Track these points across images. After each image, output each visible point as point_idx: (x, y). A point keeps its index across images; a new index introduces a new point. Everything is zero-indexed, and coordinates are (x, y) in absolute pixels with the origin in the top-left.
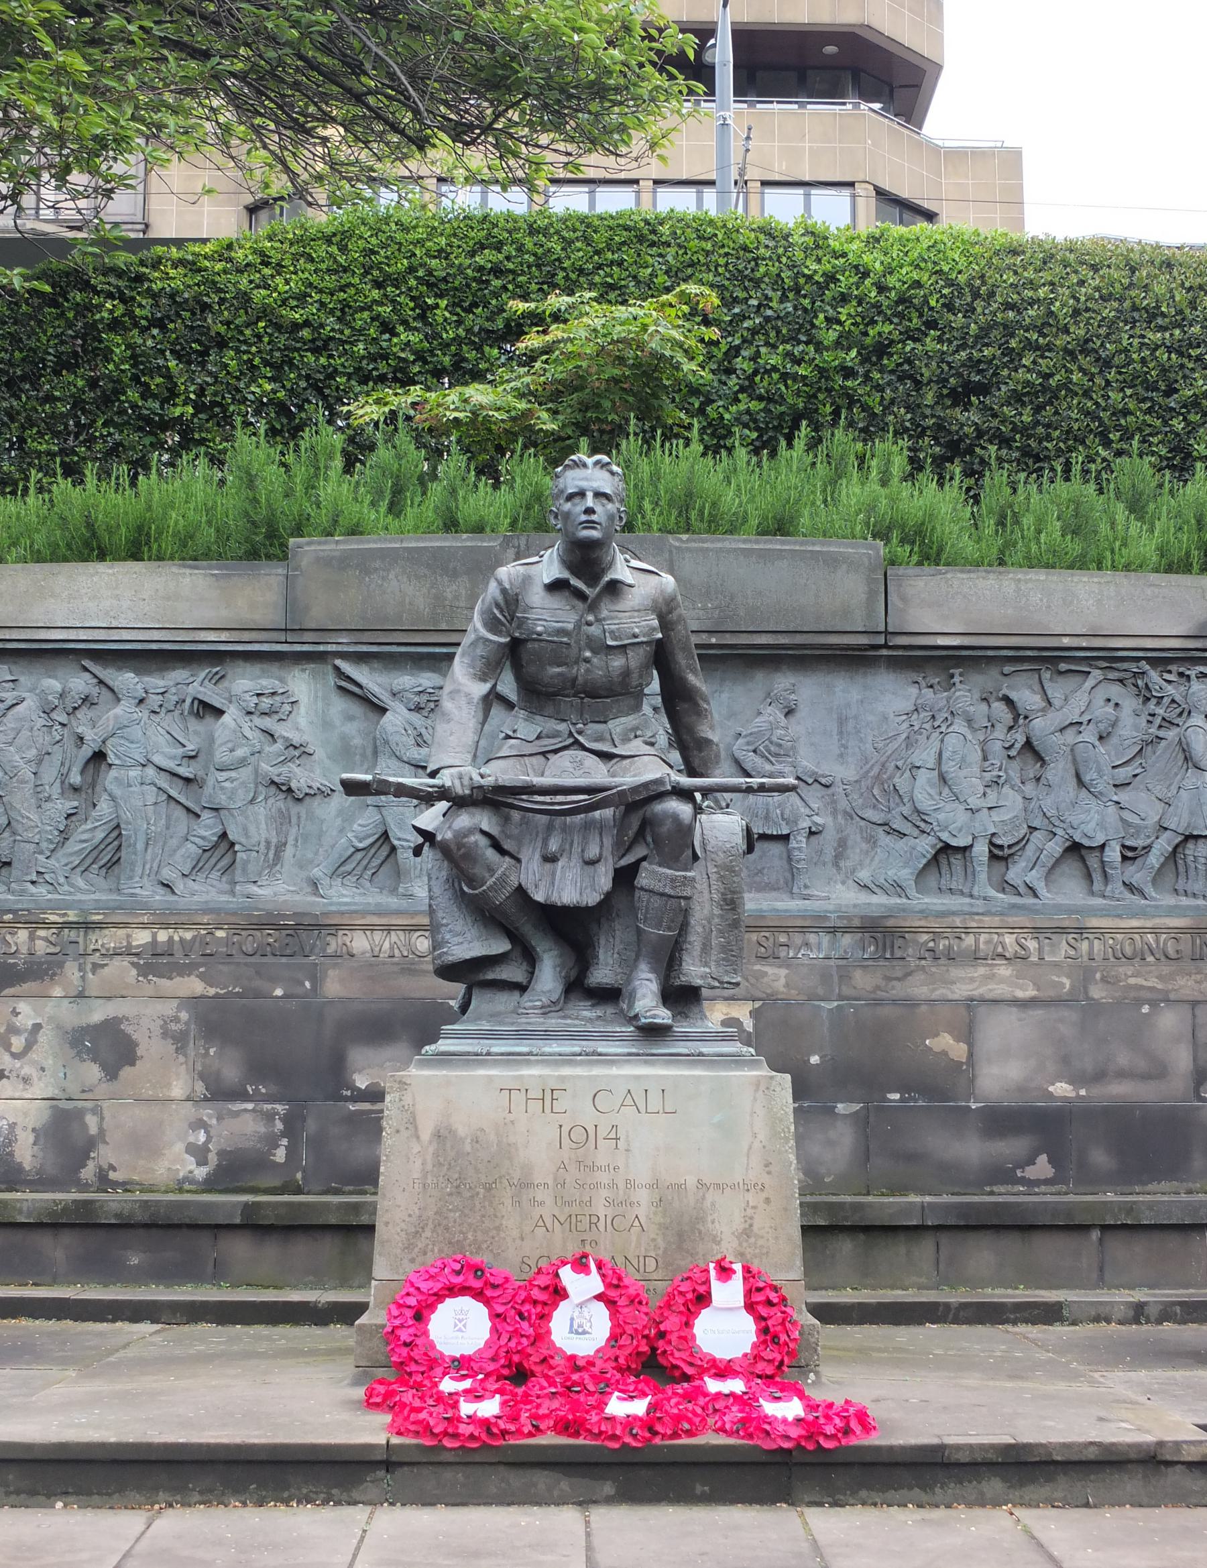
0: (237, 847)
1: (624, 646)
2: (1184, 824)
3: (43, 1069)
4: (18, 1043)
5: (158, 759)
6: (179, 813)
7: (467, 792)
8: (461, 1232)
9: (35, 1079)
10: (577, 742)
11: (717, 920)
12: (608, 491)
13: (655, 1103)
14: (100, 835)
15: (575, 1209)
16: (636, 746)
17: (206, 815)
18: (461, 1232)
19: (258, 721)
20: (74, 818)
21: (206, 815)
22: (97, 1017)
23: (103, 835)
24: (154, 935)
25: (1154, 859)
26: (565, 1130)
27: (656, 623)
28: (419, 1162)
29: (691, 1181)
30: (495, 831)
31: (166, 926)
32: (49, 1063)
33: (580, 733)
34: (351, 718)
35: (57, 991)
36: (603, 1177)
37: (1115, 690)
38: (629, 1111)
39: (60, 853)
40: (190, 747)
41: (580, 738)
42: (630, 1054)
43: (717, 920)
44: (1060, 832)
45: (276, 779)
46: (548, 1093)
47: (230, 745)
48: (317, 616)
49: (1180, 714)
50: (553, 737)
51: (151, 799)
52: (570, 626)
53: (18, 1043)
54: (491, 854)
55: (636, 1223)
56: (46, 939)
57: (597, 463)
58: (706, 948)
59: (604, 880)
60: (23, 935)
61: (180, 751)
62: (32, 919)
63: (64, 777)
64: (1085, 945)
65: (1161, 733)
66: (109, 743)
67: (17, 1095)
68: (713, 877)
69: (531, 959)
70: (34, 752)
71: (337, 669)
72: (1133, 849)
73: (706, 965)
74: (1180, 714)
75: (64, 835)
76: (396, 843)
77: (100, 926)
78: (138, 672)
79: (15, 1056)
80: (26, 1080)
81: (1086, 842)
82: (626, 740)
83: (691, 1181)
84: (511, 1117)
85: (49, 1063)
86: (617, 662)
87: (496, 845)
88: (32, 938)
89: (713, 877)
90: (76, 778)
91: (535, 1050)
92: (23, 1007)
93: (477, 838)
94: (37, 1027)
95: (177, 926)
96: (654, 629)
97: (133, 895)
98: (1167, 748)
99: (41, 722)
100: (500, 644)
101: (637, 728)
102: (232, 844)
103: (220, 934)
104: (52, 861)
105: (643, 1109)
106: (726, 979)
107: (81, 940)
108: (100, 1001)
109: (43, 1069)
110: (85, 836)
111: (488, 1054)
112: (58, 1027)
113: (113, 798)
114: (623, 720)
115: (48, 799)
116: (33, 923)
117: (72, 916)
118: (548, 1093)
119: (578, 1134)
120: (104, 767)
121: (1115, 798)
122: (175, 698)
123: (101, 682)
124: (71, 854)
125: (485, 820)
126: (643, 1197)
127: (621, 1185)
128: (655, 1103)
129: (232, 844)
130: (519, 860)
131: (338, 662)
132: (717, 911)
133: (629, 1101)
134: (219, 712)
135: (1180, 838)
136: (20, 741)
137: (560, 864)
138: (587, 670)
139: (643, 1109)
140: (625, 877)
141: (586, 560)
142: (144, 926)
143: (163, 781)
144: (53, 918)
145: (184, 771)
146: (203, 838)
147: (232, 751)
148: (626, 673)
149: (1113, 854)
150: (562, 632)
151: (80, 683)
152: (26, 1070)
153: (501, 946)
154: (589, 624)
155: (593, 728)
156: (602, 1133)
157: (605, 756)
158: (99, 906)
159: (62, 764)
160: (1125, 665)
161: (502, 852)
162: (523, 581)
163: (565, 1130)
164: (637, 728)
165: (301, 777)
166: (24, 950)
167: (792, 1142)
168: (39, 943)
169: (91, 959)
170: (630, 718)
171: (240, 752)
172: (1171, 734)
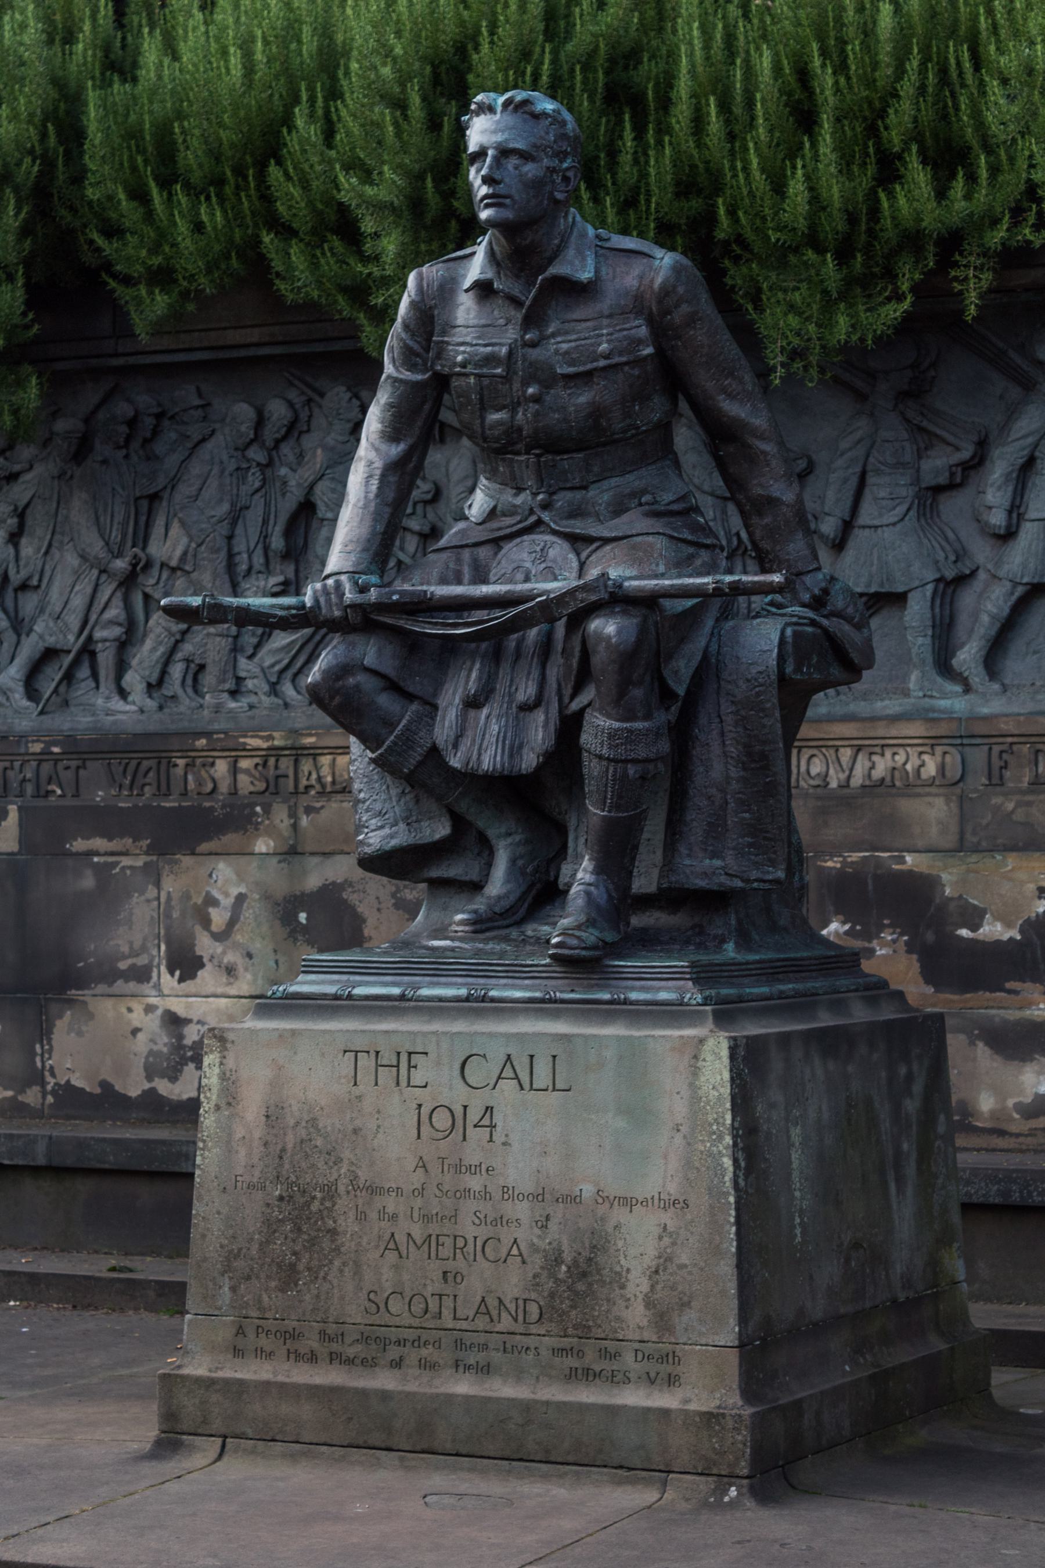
1: (589, 375)
3: (250, 956)
4: (219, 917)
7: (337, 613)
8: (295, 1253)
9: (241, 969)
10: (539, 522)
11: (734, 786)
12: (519, 145)
13: (543, 1076)
15: (434, 1229)
16: (633, 521)
18: (295, 1253)
22: (313, 882)
26: (425, 1111)
27: (643, 331)
28: (243, 1152)
29: (588, 1190)
30: (388, 667)
32: (257, 946)
33: (546, 506)
35: (262, 846)
36: (475, 1183)
38: (508, 1086)
41: (546, 517)
42: (531, 1000)
43: (734, 786)
46: (404, 1058)
47: (469, 483)
50: (512, 514)
52: (504, 350)
53: (219, 917)
54: (385, 701)
55: (515, 1251)
56: (247, 772)
57: (507, 104)
58: (716, 830)
59: (539, 733)
60: (221, 767)
62: (230, 744)
66: (319, 488)
67: (220, 990)
68: (729, 719)
69: (486, 848)
70: (225, 507)
73: (714, 855)
79: (218, 937)
80: (230, 971)
82: (618, 509)
83: (588, 1190)
84: (356, 1091)
85: (257, 946)
86: (584, 398)
87: (393, 686)
88: (234, 770)
89: (729, 719)
90: (277, 542)
91: (409, 993)
92: (224, 870)
93: (360, 678)
94: (241, 898)
96: (640, 342)
99: (232, 466)
100: (416, 385)
101: (644, 492)
105: (527, 1086)
106: (754, 874)
107: (291, 773)
108: (315, 860)
109: (250, 956)
111: (350, 997)
112: (266, 897)
114: (614, 481)
116: (235, 751)
118: (404, 1058)
119: (442, 1120)
120: (315, 524)
125: (371, 652)
126: (522, 1210)
127: (497, 1195)
128: (543, 1076)
130: (435, 707)
132: (734, 772)
133: (508, 1072)
136: (206, 494)
137: (485, 711)
138: (537, 414)
139: (527, 1086)
140: (570, 727)
141: (525, 248)
144: (253, 742)
148: (596, 413)
150: (490, 360)
152: (230, 958)
153: (440, 830)
154: (533, 345)
155: (562, 499)
156: (473, 1116)
157: (576, 540)
159: (265, 522)
161: (410, 697)
162: (442, 287)
163: (425, 1111)
164: (644, 492)
166: (224, 788)
167: (728, 1140)
168: (242, 778)
169: (304, 801)
170: (630, 477)
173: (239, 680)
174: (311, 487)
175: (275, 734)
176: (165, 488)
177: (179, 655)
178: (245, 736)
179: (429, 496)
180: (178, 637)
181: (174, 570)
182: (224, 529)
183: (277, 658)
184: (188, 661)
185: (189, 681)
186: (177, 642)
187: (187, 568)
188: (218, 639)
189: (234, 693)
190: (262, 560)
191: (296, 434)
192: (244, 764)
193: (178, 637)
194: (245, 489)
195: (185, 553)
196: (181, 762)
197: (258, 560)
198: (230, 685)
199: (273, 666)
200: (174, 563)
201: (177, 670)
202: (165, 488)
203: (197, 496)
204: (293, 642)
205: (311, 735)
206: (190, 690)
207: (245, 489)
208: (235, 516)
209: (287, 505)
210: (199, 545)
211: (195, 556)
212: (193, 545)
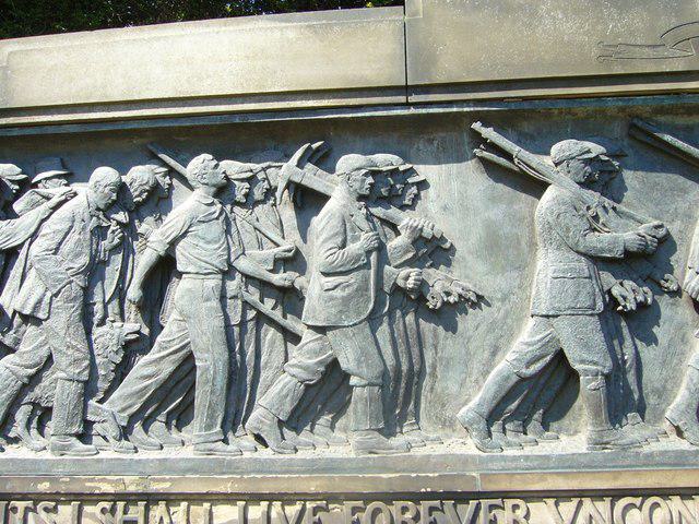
0: (353, 381)
5: (243, 264)
6: (270, 334)
14: (167, 368)
17: (308, 336)
19: (378, 211)
20: (134, 347)
21: (308, 336)
23: (171, 368)
24: (245, 510)
31: (255, 498)
34: (493, 200)
39: (115, 395)
40: (286, 245)
45: (400, 283)
47: (339, 240)
48: (448, 69)
51: (235, 319)
61: (270, 252)
62: (76, 488)
63: (120, 293)
70: (84, 260)
71: (478, 140)
75: (122, 370)
76: (577, 367)
77: (170, 499)
78: (219, 156)
90: (134, 292)
95: (271, 498)
97: (211, 452)
99: (93, 223)
102: (347, 376)
103: (335, 508)
104: (105, 406)
110: (147, 371)
113: (185, 318)
115: (102, 323)
117: (132, 485)
122: (266, 185)
123: (172, 172)
124: (131, 395)
129: (347, 376)
131: (477, 126)
134: (324, 198)
136: (65, 248)
142: (229, 498)
143: (253, 295)
145: (278, 279)
146: (306, 368)
147: (343, 246)
151: (141, 175)
158: (165, 466)
165: (442, 283)
171: (354, 248)
173: (88, 424)
174: (173, 244)
175: (127, 479)
176: (23, 244)
177: (27, 399)
178: (92, 480)
179: (291, 254)
180: (26, 380)
181: (27, 319)
182: (80, 281)
183: (129, 402)
184: (35, 405)
185: (34, 424)
186: (24, 385)
187: (41, 315)
188: (68, 383)
189: (84, 437)
190: (117, 310)
191: (156, 200)
192: (88, 509)
193: (26, 380)
194: (105, 244)
195: (40, 302)
196: (21, 505)
197: (113, 308)
198: (76, 429)
199: (123, 410)
200: (27, 311)
201: (21, 415)
202: (23, 244)
203: (57, 249)
204: (146, 387)
205: (164, 480)
206: (34, 432)
207: (105, 244)
208: (94, 271)
209: (143, 261)
210: (56, 295)
211: (50, 304)
212: (49, 294)
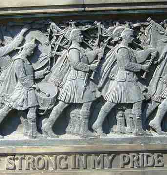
2: (68, 98)
25: (53, 116)
37: (35, 34)
44: (7, 104)
49: (67, 44)
64: (17, 163)
65: (58, 53)
72: (43, 111)
74: (67, 44)
81: (18, 108)
98: (61, 60)
121: (34, 86)
135: (67, 105)
149: (31, 114)
160: (41, 22)
172: (64, 53)
